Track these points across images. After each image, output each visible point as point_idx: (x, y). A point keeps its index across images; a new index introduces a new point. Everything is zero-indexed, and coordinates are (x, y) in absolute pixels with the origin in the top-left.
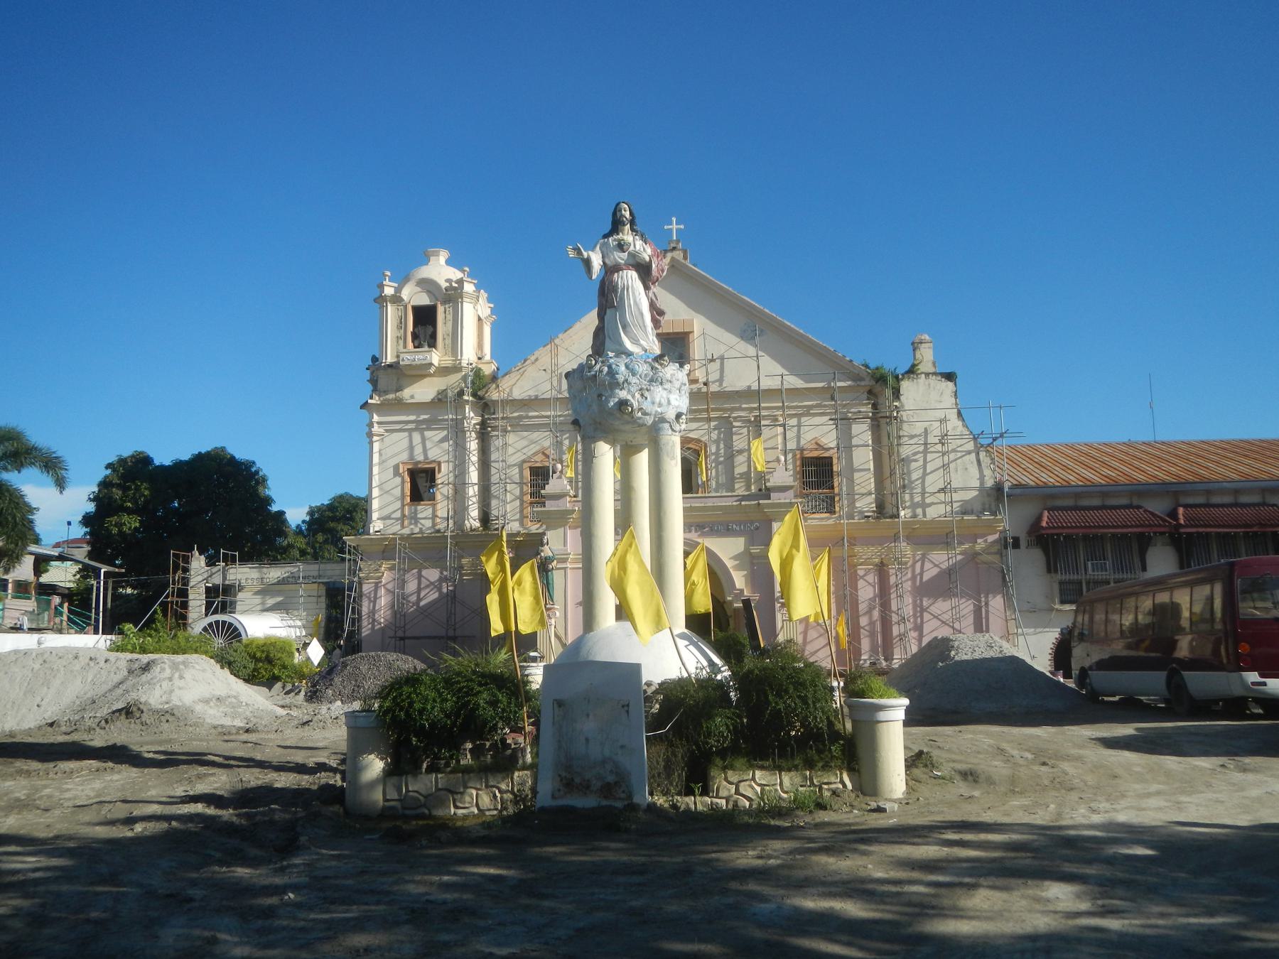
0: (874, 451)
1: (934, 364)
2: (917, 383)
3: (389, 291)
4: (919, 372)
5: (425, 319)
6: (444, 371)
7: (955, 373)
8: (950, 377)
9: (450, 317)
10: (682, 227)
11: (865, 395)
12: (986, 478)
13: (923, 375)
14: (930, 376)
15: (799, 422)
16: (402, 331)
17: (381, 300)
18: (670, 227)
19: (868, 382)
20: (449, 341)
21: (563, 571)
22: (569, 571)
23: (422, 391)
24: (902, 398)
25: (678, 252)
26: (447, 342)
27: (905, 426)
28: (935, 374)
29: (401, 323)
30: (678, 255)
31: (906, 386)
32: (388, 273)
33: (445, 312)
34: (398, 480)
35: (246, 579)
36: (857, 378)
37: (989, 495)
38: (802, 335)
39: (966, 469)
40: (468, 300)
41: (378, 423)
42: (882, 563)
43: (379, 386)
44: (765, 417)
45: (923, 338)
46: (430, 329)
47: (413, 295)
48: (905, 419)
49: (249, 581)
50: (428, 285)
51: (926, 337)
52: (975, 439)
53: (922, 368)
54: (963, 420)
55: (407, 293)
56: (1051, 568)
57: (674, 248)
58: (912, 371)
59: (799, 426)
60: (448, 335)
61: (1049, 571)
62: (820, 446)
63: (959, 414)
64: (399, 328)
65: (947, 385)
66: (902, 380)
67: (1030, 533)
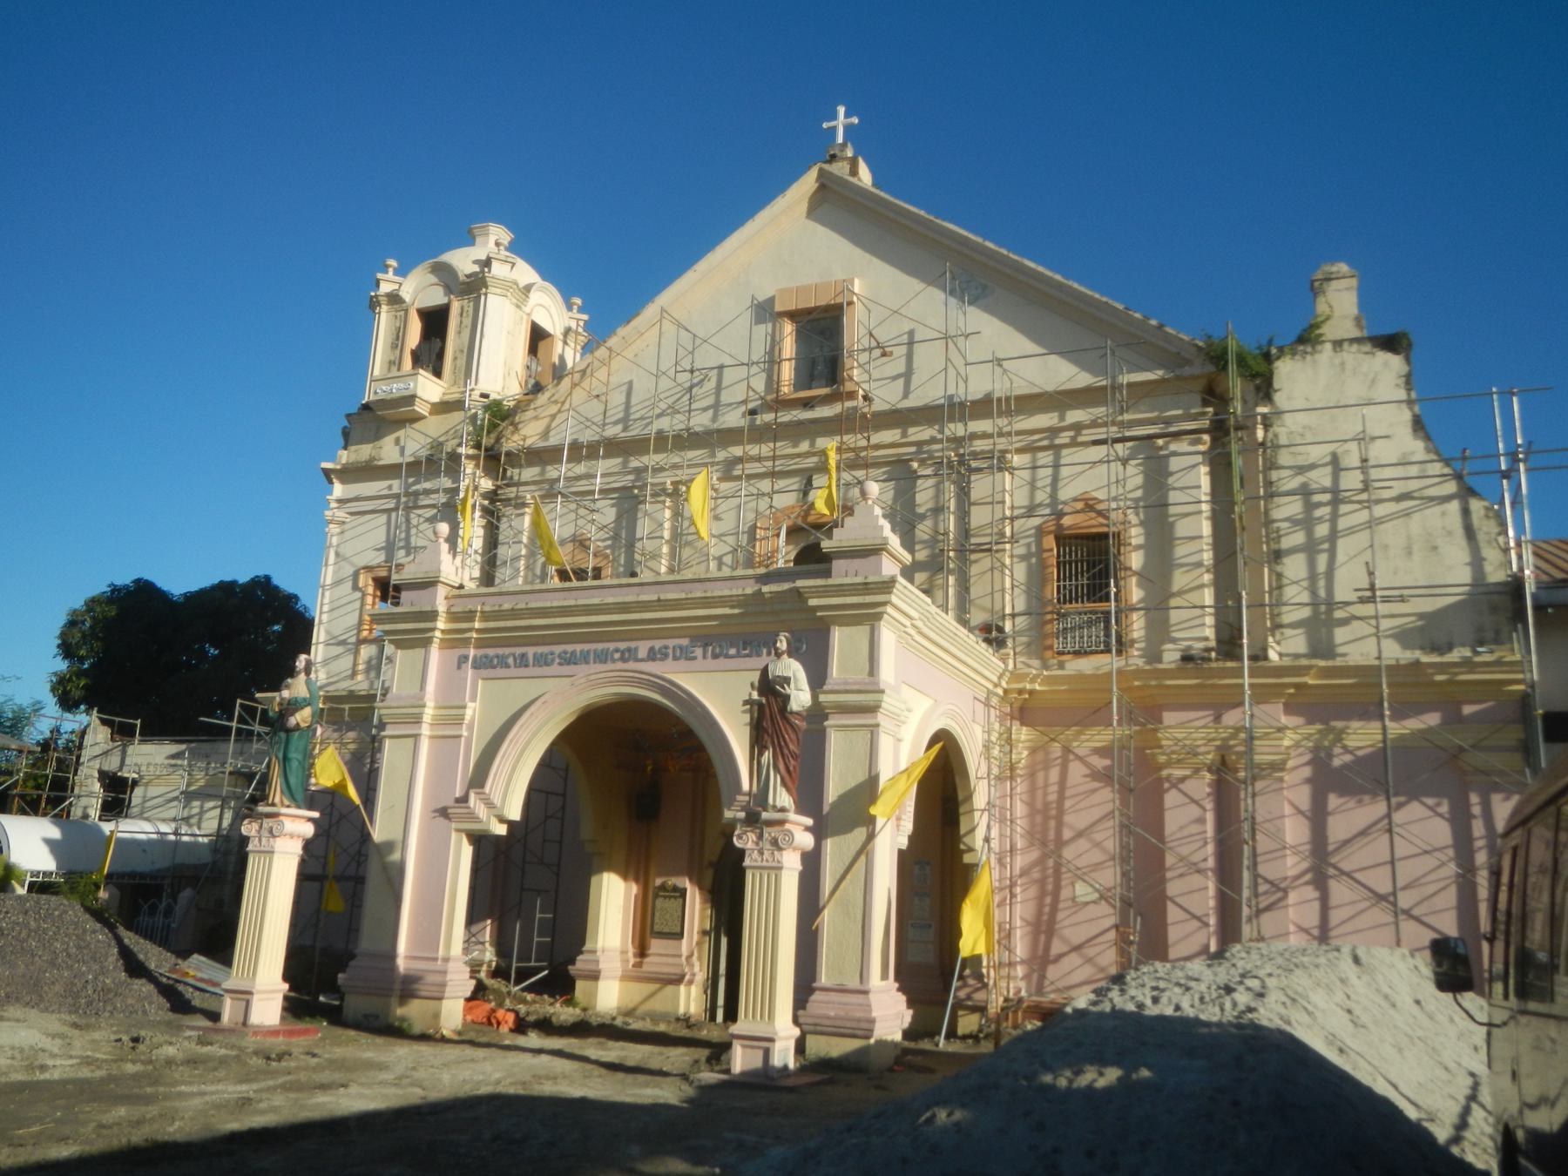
0: (1215, 518)
1: (1358, 320)
2: (1315, 362)
3: (385, 288)
4: (1324, 338)
5: (435, 322)
6: (444, 407)
7: (1405, 335)
8: (1390, 343)
9: (468, 321)
10: (855, 120)
11: (1197, 398)
12: (1488, 568)
13: (1328, 346)
14: (1346, 345)
15: (1057, 457)
16: (398, 352)
17: (374, 304)
18: (832, 124)
19: (1201, 368)
20: (462, 362)
21: (411, 740)
22: (425, 746)
23: (410, 444)
24: (1277, 397)
25: (840, 164)
26: (458, 362)
27: (1284, 458)
28: (1353, 341)
29: (398, 338)
30: (840, 169)
31: (1287, 371)
32: (393, 263)
33: (461, 315)
34: (358, 595)
35: (149, 764)
36: (1173, 358)
37: (1494, 609)
38: (1060, 286)
39: (1435, 548)
40: (499, 291)
41: (342, 501)
42: (1223, 762)
44: (975, 455)
45: (1334, 269)
47: (419, 289)
48: (1283, 440)
49: (151, 768)
50: (445, 273)
51: (1343, 268)
52: (1458, 477)
53: (1330, 331)
54: (1427, 438)
55: (411, 290)
57: (833, 158)
58: (1307, 338)
59: (1056, 466)
60: (462, 351)
62: (1089, 505)
63: (1418, 425)
64: (394, 346)
65: (1386, 364)
66: (1278, 358)
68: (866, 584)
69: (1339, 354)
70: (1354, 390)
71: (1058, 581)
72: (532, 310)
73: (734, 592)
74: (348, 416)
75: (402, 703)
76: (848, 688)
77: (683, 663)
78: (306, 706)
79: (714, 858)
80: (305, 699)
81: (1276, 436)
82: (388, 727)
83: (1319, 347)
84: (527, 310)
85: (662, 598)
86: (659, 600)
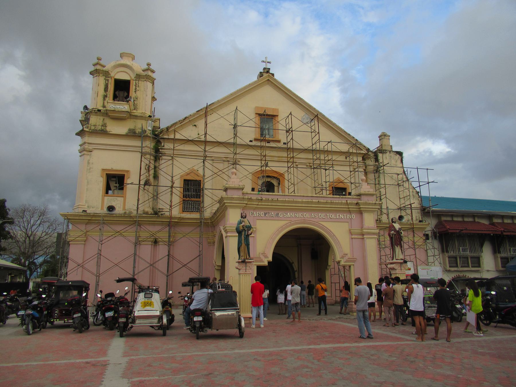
46: (126, 94)
56: (444, 249)
61: (443, 251)
65: (398, 157)
68: (375, 203)
73: (339, 202)
76: (369, 228)
83: (387, 151)
85: (319, 201)
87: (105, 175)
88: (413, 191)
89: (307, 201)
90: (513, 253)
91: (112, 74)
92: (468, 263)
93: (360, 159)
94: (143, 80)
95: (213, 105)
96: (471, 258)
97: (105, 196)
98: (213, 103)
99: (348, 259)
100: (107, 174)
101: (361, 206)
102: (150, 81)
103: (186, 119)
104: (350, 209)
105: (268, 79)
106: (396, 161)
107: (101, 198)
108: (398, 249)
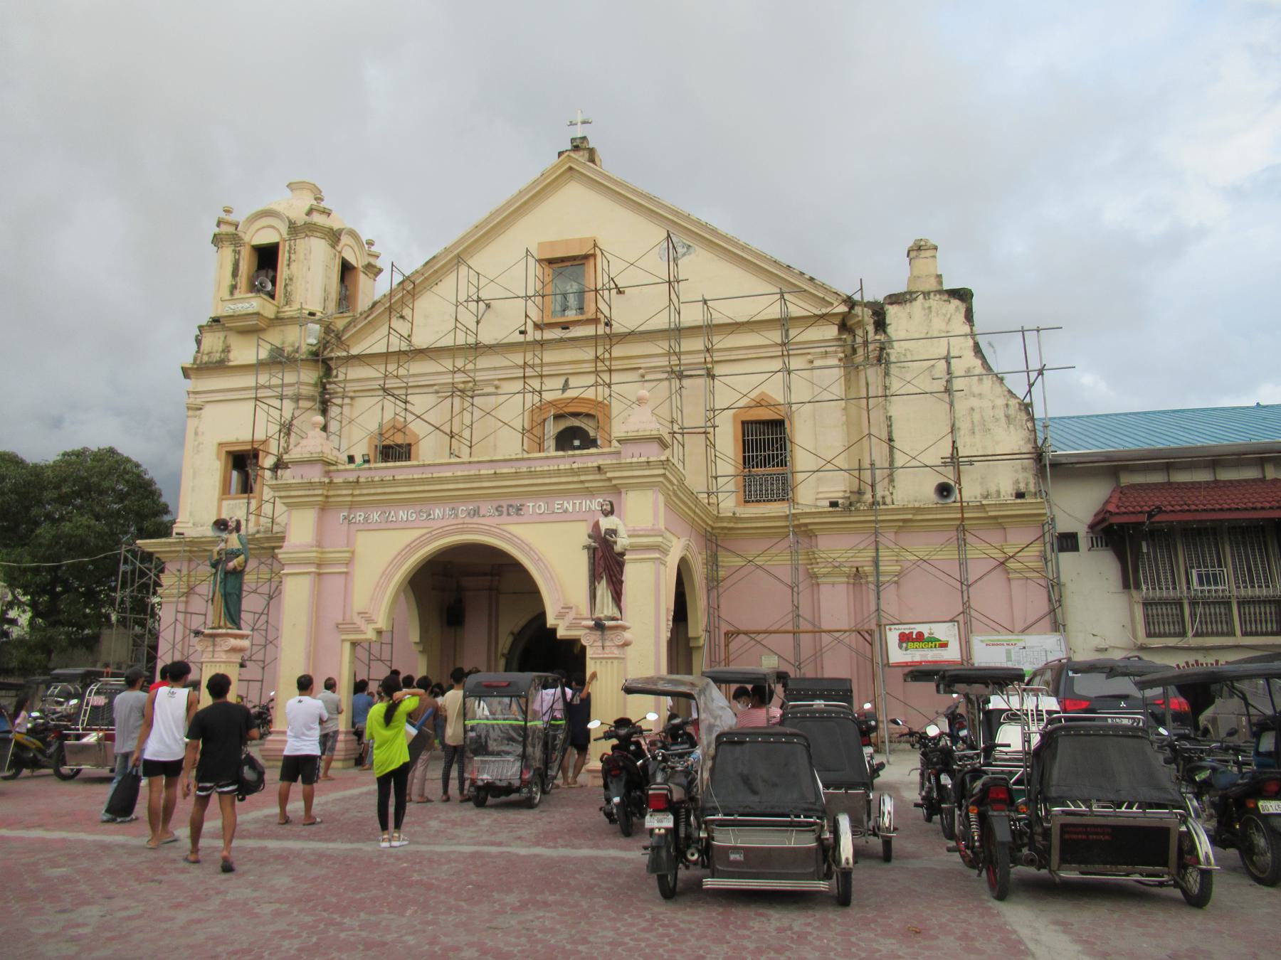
14: (932, 294)
24: (890, 330)
43: (201, 350)
46: (271, 274)
56: (1129, 582)
61: (1126, 586)
65: (957, 308)
67: (1092, 527)
68: (648, 462)
69: (928, 301)
70: (938, 325)
71: (744, 452)
72: (342, 249)
73: (552, 468)
74: (201, 328)
75: (297, 550)
76: (636, 533)
77: (515, 518)
78: (240, 555)
79: (505, 651)
80: (238, 550)
81: (888, 354)
82: (286, 567)
83: (914, 296)
84: (339, 248)
85: (498, 472)
86: (495, 473)
87: (223, 455)
88: (1007, 405)
89: (466, 473)
90: (1201, 583)
91: (247, 238)
92: (1230, 621)
93: (832, 331)
94: (303, 235)
95: (436, 260)
96: (1242, 603)
97: (223, 499)
98: (434, 258)
99: (574, 621)
100: (229, 453)
101: (609, 475)
102: (319, 234)
103: (377, 306)
104: (587, 485)
105: (567, 166)
106: (949, 320)
107: (216, 503)
108: (603, 588)
